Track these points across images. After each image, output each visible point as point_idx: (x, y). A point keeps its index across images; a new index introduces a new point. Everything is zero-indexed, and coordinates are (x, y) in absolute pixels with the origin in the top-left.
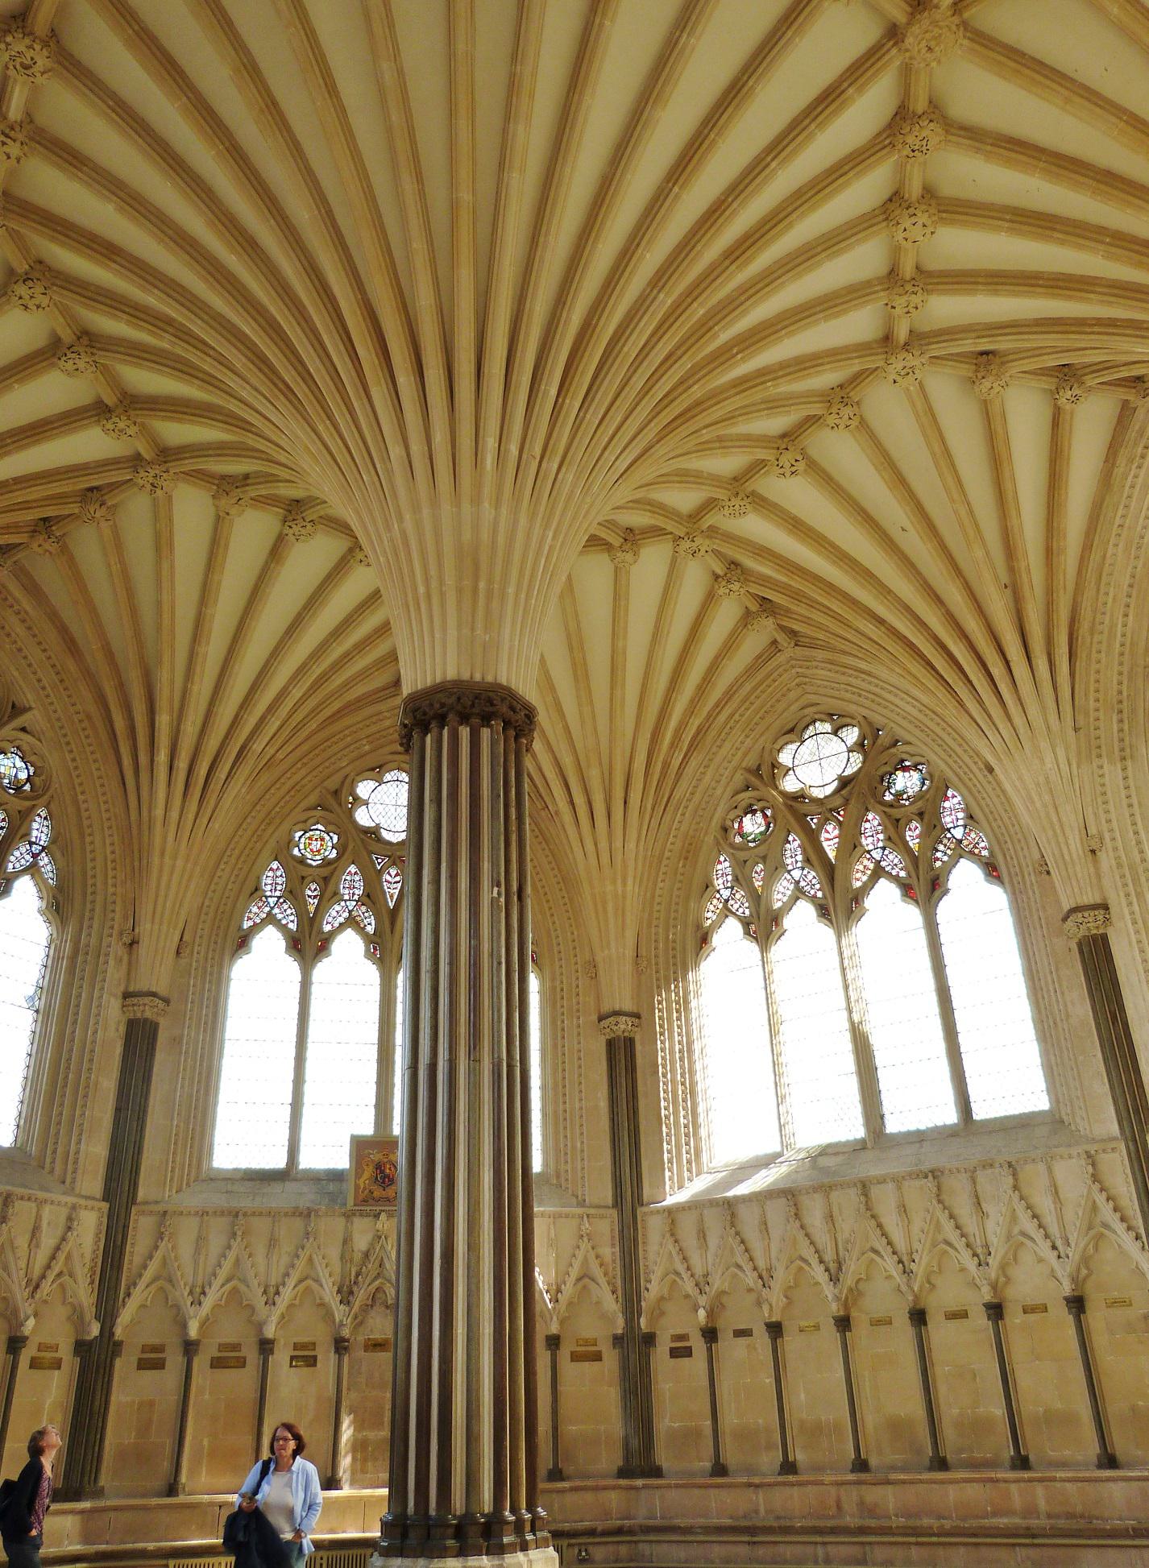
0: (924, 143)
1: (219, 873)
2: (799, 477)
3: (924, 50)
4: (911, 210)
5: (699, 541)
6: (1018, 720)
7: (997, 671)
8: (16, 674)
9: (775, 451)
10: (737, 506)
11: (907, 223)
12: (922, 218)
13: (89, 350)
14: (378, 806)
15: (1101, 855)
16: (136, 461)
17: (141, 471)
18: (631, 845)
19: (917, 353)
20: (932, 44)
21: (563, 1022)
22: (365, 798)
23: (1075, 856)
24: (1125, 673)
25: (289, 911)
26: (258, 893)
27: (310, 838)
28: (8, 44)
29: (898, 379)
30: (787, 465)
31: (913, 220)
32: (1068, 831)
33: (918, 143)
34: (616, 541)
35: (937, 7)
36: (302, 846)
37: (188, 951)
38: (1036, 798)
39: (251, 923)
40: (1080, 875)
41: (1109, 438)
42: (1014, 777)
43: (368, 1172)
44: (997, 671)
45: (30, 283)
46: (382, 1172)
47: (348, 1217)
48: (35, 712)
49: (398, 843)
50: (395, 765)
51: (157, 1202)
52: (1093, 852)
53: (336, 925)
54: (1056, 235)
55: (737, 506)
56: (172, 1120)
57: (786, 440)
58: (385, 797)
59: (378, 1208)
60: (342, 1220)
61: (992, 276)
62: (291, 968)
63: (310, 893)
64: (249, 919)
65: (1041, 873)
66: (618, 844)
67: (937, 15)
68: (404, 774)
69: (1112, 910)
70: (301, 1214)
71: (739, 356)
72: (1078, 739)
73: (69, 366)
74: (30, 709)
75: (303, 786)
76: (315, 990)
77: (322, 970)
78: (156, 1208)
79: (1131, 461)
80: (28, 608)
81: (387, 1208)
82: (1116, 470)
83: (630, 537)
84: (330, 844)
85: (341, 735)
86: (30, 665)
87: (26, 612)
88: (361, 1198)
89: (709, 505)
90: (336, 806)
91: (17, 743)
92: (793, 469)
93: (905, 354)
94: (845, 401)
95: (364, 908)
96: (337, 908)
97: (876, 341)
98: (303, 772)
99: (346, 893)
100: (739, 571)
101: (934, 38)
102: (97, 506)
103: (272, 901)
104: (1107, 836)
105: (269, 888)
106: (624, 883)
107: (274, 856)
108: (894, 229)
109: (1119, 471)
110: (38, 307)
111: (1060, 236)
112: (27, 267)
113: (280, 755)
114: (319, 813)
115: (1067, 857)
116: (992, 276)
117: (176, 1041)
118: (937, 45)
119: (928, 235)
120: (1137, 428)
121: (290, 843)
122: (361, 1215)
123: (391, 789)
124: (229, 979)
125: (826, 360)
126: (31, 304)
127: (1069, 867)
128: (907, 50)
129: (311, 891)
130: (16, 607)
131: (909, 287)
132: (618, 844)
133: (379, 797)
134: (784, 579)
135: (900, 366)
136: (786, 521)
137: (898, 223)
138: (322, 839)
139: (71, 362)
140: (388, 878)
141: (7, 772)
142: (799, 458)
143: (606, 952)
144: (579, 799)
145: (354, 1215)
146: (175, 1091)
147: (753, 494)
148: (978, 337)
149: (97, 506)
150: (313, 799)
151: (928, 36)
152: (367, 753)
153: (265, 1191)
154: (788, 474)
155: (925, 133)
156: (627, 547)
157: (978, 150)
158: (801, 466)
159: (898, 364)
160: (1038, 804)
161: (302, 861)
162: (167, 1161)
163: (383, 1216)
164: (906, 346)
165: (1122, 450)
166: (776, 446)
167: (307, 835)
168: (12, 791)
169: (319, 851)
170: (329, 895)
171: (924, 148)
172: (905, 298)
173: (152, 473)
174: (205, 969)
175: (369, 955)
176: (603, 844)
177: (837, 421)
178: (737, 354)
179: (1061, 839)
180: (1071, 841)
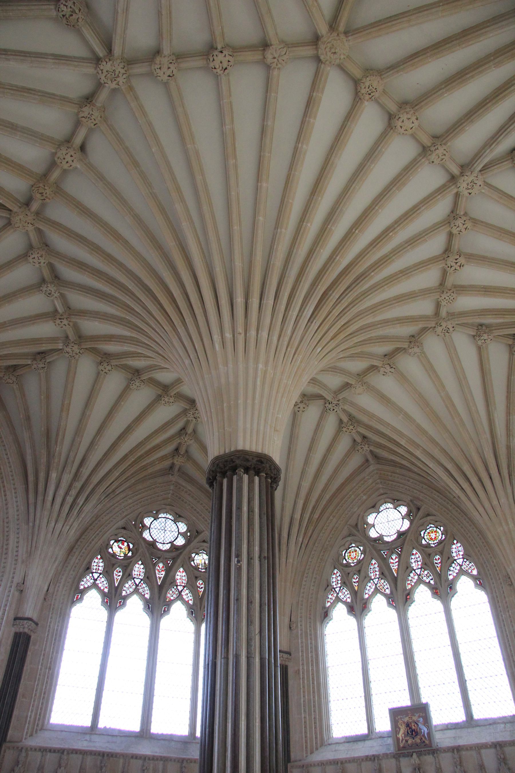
0: (371, 87)
1: (304, 583)
2: (465, 266)
3: (332, 55)
4: (397, 117)
5: (444, 324)
8: (194, 518)
9: (443, 261)
11: (399, 123)
12: (404, 117)
13: (138, 377)
14: (380, 524)
16: (185, 412)
17: (187, 414)
18: (503, 500)
19: (469, 173)
20: (333, 51)
21: (502, 616)
22: (372, 523)
25: (346, 593)
26: (330, 587)
27: (350, 552)
28: (41, 290)
29: (470, 191)
31: (401, 120)
33: (369, 90)
34: (406, 345)
35: (322, 36)
36: (346, 558)
37: (295, 625)
39: (329, 604)
43: (403, 730)
45: (102, 364)
46: (410, 728)
47: (396, 758)
48: (206, 532)
49: (392, 541)
50: (383, 501)
51: (300, 760)
53: (370, 593)
54: (468, 76)
56: (301, 714)
57: (447, 253)
58: (382, 519)
59: (411, 751)
60: (393, 761)
61: (467, 116)
62: (352, 621)
63: (354, 580)
64: (328, 602)
66: (495, 502)
67: (324, 39)
68: (389, 504)
70: (370, 759)
71: (357, 231)
73: (135, 387)
74: (204, 531)
75: (337, 528)
76: (367, 631)
77: (369, 620)
78: (300, 763)
80: (190, 489)
81: (416, 750)
83: (413, 339)
84: (360, 552)
85: (348, 496)
86: (198, 513)
87: (189, 490)
88: (401, 745)
89: (438, 306)
90: (356, 532)
91: (202, 548)
92: (459, 264)
93: (463, 178)
94: (455, 218)
95: (382, 581)
96: (369, 584)
97: (448, 181)
98: (335, 520)
99: (372, 575)
100: (484, 328)
101: (331, 48)
102: (184, 436)
103: (337, 590)
105: (334, 583)
106: (507, 524)
107: (333, 567)
108: (396, 130)
110: (109, 371)
111: (471, 74)
112: (100, 358)
113: (316, 516)
114: (349, 539)
116: (467, 116)
117: (298, 672)
119: (415, 121)
121: (339, 557)
122: (403, 756)
123: (384, 514)
124: (323, 635)
125: (421, 205)
126: (106, 371)
128: (326, 61)
129: (355, 579)
130: (185, 490)
131: (433, 149)
132: (495, 502)
133: (379, 520)
134: (501, 321)
135: (465, 185)
136: (479, 291)
137: (395, 127)
138: (356, 551)
139: (134, 385)
140: (392, 561)
141: (200, 563)
142: (458, 257)
143: (511, 567)
144: (465, 485)
145: (400, 756)
146: (300, 698)
147: (455, 286)
148: (491, 146)
149: (184, 436)
150: (345, 532)
151: (328, 50)
152: (366, 500)
153: (353, 748)
154: (458, 268)
155: (367, 84)
156: (412, 346)
157: (398, 72)
158: (462, 260)
159: (463, 184)
161: (348, 565)
162: (302, 737)
163: (414, 754)
164: (462, 174)
166: (442, 258)
167: (348, 551)
168: (203, 570)
169: (355, 557)
170: (366, 579)
171: (374, 90)
172: (434, 154)
173: (191, 413)
174: (306, 633)
175: (390, 604)
176: (487, 505)
177: (458, 229)
178: (356, 230)
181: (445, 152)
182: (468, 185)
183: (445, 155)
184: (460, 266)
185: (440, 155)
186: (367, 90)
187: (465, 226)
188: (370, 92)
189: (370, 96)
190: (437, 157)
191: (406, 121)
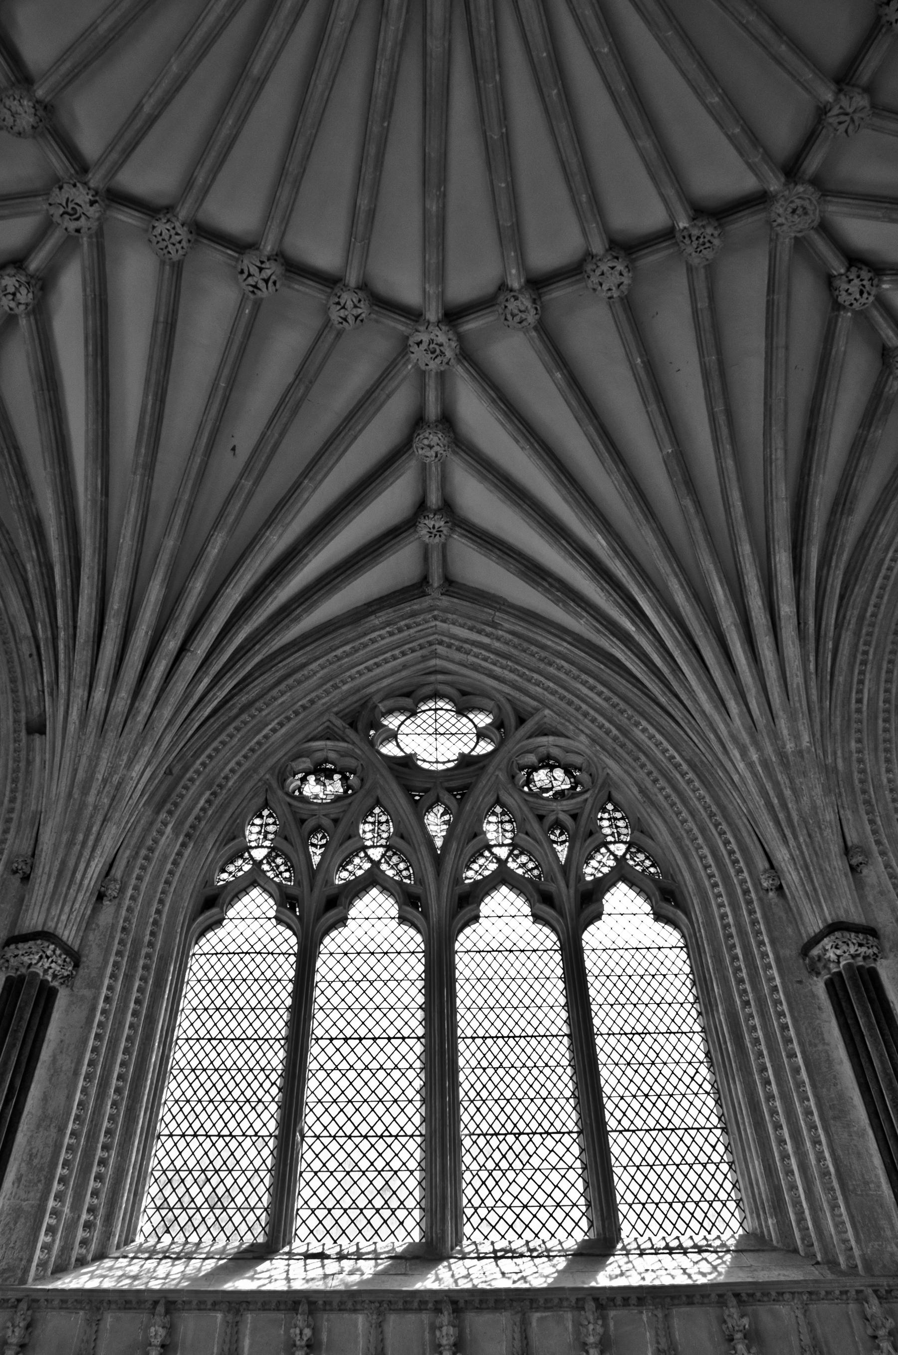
0: (708, 245)
3: (793, 206)
6: (145, 707)
7: (171, 644)
10: (178, 238)
15: (108, 907)
20: (799, 211)
23: (86, 882)
24: (243, 769)
30: (266, 274)
32: (98, 852)
38: (93, 792)
40: (77, 906)
41: (384, 593)
42: (87, 750)
44: (171, 644)
52: (101, 897)
55: (178, 238)
65: (15, 872)
69: (82, 972)
72: (161, 782)
79: (388, 624)
82: (373, 617)
104: (130, 892)
109: (374, 620)
115: (78, 876)
118: (800, 216)
120: (415, 607)
127: (74, 887)
135: (442, 338)
160: (91, 799)
165: (390, 610)
179: (87, 853)
180: (93, 864)
181: (509, 317)
182: (441, 345)
183: (520, 323)
184: (255, 287)
185: (524, 316)
186: (708, 238)
187: (351, 319)
188: (701, 240)
189: (694, 239)
190: (523, 308)
191: (619, 279)
